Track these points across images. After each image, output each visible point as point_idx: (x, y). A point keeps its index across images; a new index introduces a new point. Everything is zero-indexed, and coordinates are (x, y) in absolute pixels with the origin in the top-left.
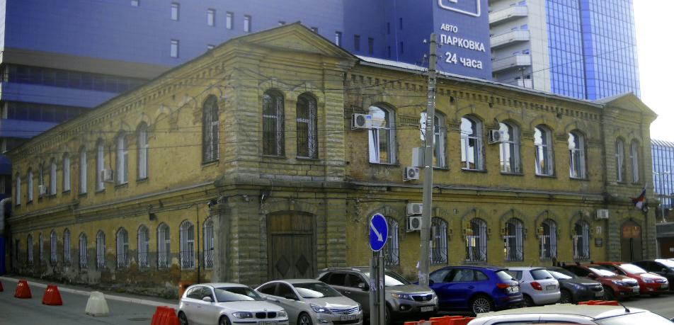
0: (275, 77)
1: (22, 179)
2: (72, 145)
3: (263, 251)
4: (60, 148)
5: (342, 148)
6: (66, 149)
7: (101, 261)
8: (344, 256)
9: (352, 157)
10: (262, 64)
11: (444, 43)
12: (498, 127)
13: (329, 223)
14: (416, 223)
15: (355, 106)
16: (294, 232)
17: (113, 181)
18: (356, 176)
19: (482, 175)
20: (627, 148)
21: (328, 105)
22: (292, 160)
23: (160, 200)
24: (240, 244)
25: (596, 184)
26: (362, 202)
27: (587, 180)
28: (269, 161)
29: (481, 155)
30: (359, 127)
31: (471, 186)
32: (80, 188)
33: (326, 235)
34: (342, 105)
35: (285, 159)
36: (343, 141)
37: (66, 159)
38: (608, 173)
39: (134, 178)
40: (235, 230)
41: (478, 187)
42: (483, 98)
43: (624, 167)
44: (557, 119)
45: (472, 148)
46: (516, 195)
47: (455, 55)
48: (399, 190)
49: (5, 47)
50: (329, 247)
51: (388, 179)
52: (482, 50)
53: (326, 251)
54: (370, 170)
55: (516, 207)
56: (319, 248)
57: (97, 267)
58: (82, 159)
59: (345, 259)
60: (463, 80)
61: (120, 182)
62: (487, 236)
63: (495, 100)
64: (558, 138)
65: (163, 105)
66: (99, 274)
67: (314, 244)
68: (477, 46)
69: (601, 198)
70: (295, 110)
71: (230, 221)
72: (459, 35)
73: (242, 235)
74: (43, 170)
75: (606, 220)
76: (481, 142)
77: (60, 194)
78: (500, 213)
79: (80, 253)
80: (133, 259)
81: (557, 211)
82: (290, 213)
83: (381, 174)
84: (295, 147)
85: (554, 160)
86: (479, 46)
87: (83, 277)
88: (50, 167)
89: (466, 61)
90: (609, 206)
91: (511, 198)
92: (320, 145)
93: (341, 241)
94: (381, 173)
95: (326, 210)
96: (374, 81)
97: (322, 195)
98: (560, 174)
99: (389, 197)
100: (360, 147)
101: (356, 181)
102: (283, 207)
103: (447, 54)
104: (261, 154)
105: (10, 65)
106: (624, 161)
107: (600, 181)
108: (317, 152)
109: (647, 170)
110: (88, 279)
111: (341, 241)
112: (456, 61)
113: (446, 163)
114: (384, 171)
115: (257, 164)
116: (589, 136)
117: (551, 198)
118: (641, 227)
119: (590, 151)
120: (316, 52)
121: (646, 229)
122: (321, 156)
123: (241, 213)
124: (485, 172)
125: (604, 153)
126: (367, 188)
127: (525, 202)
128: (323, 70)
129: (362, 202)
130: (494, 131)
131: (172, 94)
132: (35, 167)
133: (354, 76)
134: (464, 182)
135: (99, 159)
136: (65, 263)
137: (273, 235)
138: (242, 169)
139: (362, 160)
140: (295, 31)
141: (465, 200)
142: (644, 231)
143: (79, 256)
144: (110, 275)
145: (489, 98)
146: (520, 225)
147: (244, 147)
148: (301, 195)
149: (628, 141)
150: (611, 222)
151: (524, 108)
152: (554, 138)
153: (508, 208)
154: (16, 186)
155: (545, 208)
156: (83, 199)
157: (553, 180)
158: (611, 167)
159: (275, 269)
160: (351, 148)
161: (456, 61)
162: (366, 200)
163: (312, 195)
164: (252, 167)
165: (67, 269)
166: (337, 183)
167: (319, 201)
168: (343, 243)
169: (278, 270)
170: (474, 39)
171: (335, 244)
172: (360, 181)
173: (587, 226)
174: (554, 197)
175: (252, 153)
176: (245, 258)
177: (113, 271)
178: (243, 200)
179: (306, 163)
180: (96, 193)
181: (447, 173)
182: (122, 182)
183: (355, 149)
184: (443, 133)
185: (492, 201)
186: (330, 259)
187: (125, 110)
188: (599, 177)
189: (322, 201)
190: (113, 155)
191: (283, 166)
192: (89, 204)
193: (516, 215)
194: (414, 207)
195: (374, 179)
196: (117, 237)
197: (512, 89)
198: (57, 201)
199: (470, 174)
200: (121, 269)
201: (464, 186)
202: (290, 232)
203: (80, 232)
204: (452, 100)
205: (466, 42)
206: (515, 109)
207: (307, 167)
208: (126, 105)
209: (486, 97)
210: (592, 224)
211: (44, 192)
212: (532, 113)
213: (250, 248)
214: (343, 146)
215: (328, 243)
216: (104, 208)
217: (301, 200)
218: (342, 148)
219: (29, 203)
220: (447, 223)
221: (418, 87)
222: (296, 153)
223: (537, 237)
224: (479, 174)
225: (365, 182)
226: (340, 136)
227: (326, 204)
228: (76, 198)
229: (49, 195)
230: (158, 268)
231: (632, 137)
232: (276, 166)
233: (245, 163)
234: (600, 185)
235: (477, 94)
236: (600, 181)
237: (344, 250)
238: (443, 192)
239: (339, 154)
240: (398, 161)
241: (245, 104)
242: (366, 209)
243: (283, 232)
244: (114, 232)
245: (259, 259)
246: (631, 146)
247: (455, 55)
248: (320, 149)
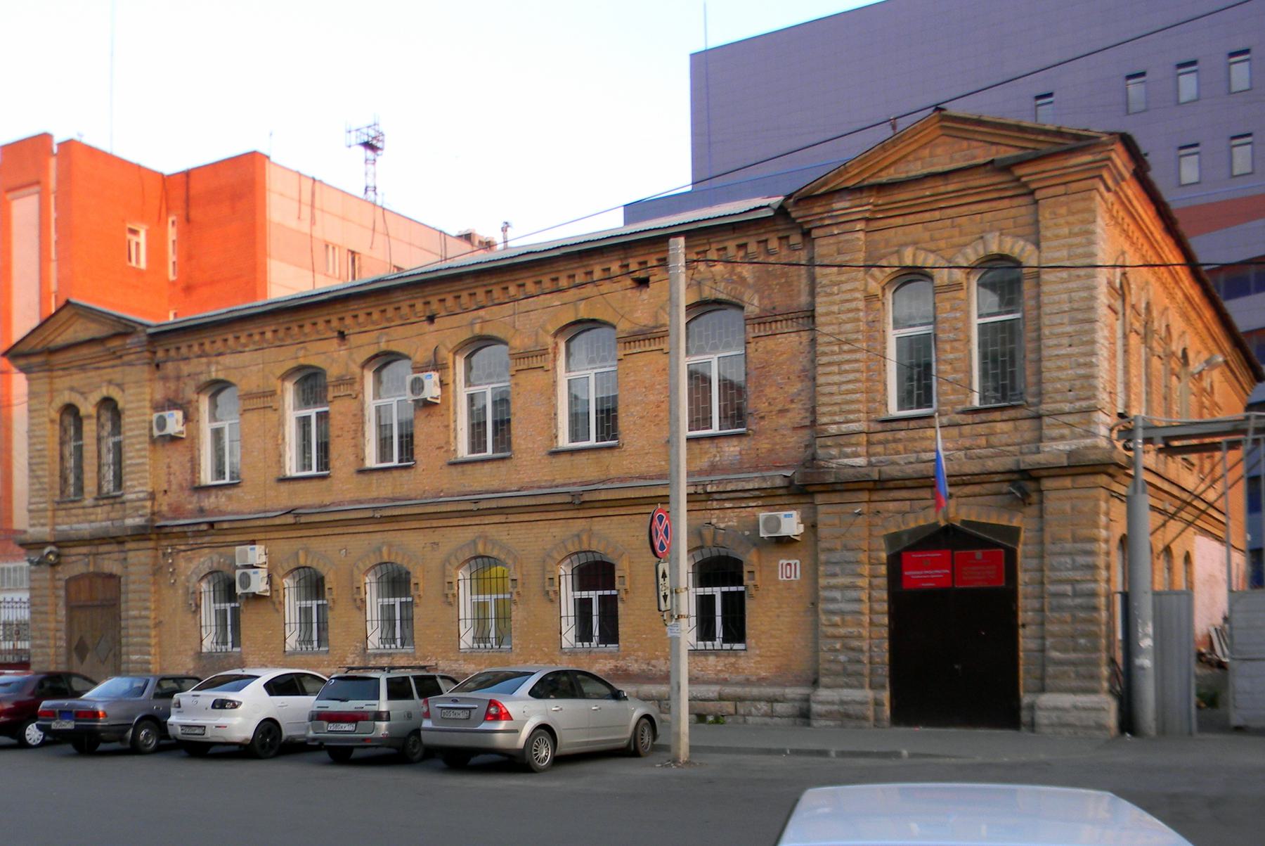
9: (169, 482)
26: (184, 551)
46: (474, 507)
48: (225, 526)
51: (221, 509)
54: (195, 499)
83: (210, 502)
94: (213, 499)
104: (57, 499)
126: (178, 529)
127: (512, 518)
129: (184, 551)
134: (362, 495)
139: (184, 485)
141: (362, 529)
160: (169, 467)
162: (189, 547)
163: (114, 547)
164: (41, 518)
181: (329, 479)
183: (175, 467)
195: (201, 511)
201: (360, 502)
214: (147, 467)
218: (146, 471)
226: (143, 453)
239: (141, 481)
242: (189, 560)
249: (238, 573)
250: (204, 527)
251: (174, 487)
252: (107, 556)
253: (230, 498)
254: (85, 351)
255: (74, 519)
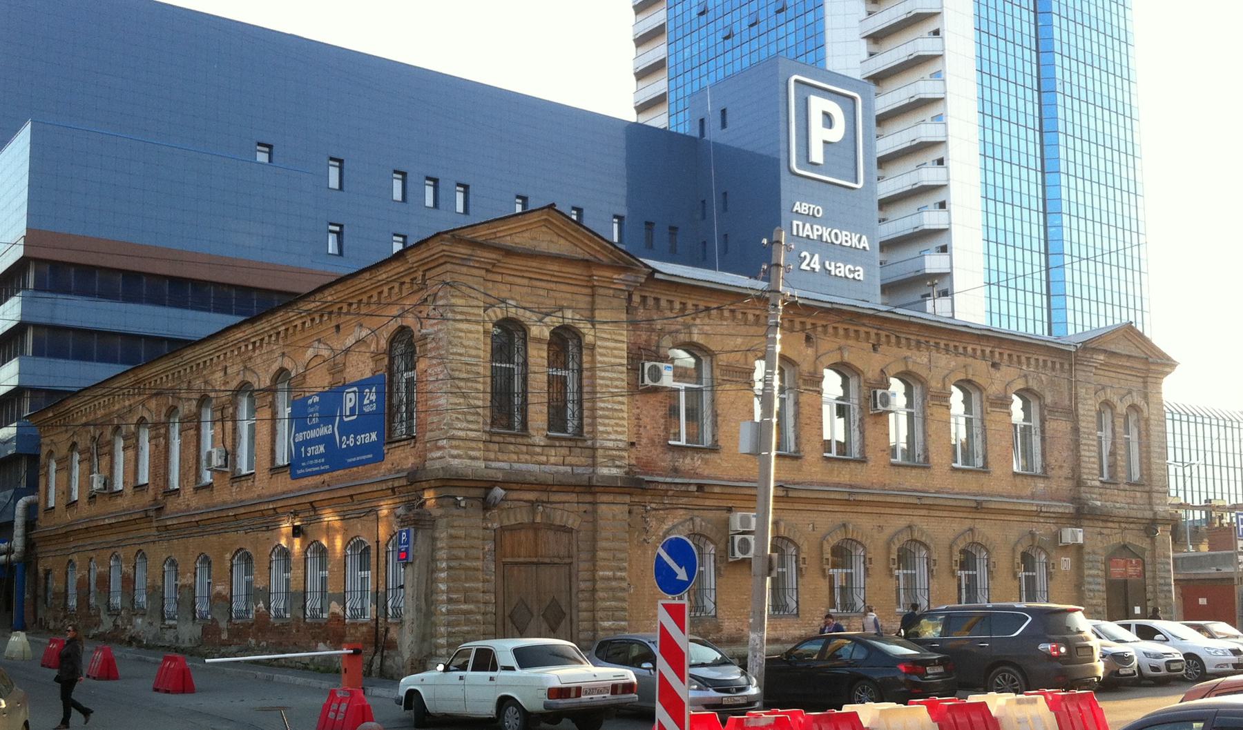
0: (512, 299)
1: (58, 462)
2: (153, 404)
3: (489, 592)
4: (131, 410)
5: (623, 418)
6: (141, 412)
7: (202, 607)
8: (624, 600)
9: (638, 435)
10: (490, 276)
11: (798, 235)
12: (887, 386)
13: (602, 544)
14: (745, 546)
15: (644, 349)
16: (541, 560)
17: (227, 470)
18: (647, 466)
19: (859, 466)
20: (1120, 422)
21: (600, 347)
22: (539, 439)
23: (311, 503)
24: (450, 579)
25: (1060, 483)
26: (655, 509)
27: (1045, 476)
28: (501, 439)
29: (857, 433)
30: (651, 384)
31: (838, 485)
32: (167, 481)
33: (594, 565)
34: (625, 346)
35: (528, 436)
36: (625, 408)
37: (141, 430)
38: (1083, 465)
39: (268, 465)
40: (442, 554)
41: (851, 487)
42: (862, 335)
43: (1113, 454)
44: (992, 370)
45: (842, 420)
46: (917, 501)
47: (816, 257)
48: (717, 490)
49: (28, 229)
50: (599, 585)
52: (864, 248)
53: (594, 590)
54: (669, 456)
55: (917, 521)
56: (583, 585)
57: (194, 618)
58: (171, 430)
59: (625, 605)
60: (829, 306)
61: (240, 470)
62: (866, 570)
63: (883, 339)
64: (993, 404)
65: (319, 341)
66: (198, 630)
67: (574, 579)
68: (855, 240)
69: (1069, 508)
70: (545, 354)
71: (434, 539)
72: (823, 222)
73: (453, 564)
74: (99, 447)
75: (1079, 548)
76: (857, 411)
77: (129, 490)
78: (889, 531)
79: (163, 592)
80: (261, 605)
81: (988, 530)
82: (534, 527)
83: (686, 463)
84: (545, 417)
85: (985, 441)
86: (859, 241)
87: (169, 636)
88: (111, 444)
89: (836, 267)
90: (1086, 523)
91: (905, 506)
92: (586, 413)
93: (619, 574)
94: (688, 460)
95: (595, 521)
96: (677, 306)
97: (589, 498)
98: (994, 467)
99: (700, 502)
100: (653, 416)
101: (646, 474)
102: (523, 517)
103: (803, 255)
104: (488, 428)
105: (39, 261)
106: (1114, 443)
107: (1066, 478)
108: (580, 427)
109: (1155, 460)
110: (177, 638)
111: (619, 574)
112: (817, 267)
113: (797, 445)
114: (692, 459)
115: (481, 445)
116: (1049, 400)
117: (978, 508)
118: (1144, 561)
119: (1051, 425)
120: (581, 257)
121: (1154, 563)
122: (588, 433)
123: (453, 527)
124: (863, 461)
125: (1076, 430)
126: (664, 487)
127: (933, 513)
128: (593, 287)
129: (655, 509)
130: (879, 392)
131: (334, 323)
132: (84, 441)
133: (644, 299)
134: (827, 478)
135: (203, 431)
136: (134, 610)
137: (505, 564)
138: (455, 452)
139: (657, 440)
140: (546, 220)
142: (1148, 568)
143: (163, 599)
144: (218, 631)
145: (873, 336)
146: (924, 553)
147: (460, 416)
148: (555, 498)
149: (1121, 408)
150: (1087, 549)
151: (934, 354)
152: (986, 404)
153: (902, 522)
154: (47, 474)
155: (968, 524)
156: (170, 499)
157: (982, 476)
158: (1088, 455)
159: (508, 621)
161: (817, 267)
162: (662, 507)
163: (572, 497)
164: (473, 449)
165: (139, 621)
166: (615, 478)
167: (583, 507)
168: (622, 579)
169: (513, 623)
170: (852, 228)
171: (608, 579)
172: (652, 475)
173: (1043, 557)
174: (984, 505)
175: (471, 426)
176: (457, 601)
177: (223, 624)
178: (457, 504)
179: (564, 443)
180: (197, 489)
182: (245, 471)
183: (645, 420)
184: (791, 395)
185: (875, 510)
186: (601, 604)
187: (250, 347)
188: (1066, 471)
189: (588, 507)
190: (229, 425)
191: (524, 449)
192: (183, 507)
193: (916, 535)
194: (742, 518)
195: (676, 471)
196: (232, 566)
197: (912, 319)
198: (123, 503)
199: (836, 465)
200: (238, 621)
202: (535, 560)
203: (165, 556)
204: (808, 339)
205: (836, 234)
206: (917, 353)
207: (565, 451)
208: (253, 340)
209: (867, 333)
210: (1053, 554)
211: (100, 486)
212: (945, 362)
213: (467, 585)
214: (625, 415)
215: (597, 578)
216: (211, 516)
217: (554, 506)
218: (623, 418)
219: (72, 504)
220: (798, 548)
221: (751, 317)
222: (546, 427)
223: (953, 573)
224: (852, 465)
225: (661, 475)
226: (620, 399)
227: (595, 511)
228: (160, 498)
229: (109, 491)
230: (305, 618)
231: (1128, 401)
232: (512, 447)
233: (461, 443)
234: (1067, 485)
235: (852, 328)
236: (1066, 478)
237: (623, 590)
238: (791, 494)
239: (619, 429)
240: (717, 441)
241: (461, 343)
242: (662, 521)
243: (521, 560)
244: (228, 556)
245: (481, 606)
246: (1126, 417)
247: (816, 257)
248: (586, 421)
249: (738, 538)
250: (693, 488)
251: (644, 441)
252: (561, 506)
253: (706, 462)
254: (554, 267)
255: (515, 457)
